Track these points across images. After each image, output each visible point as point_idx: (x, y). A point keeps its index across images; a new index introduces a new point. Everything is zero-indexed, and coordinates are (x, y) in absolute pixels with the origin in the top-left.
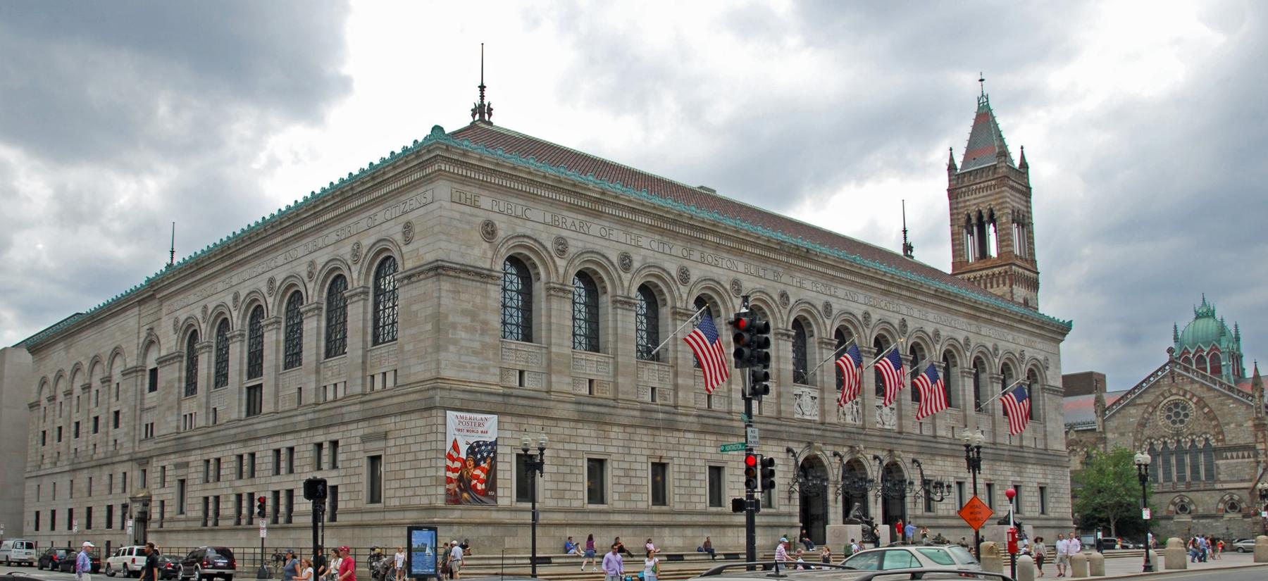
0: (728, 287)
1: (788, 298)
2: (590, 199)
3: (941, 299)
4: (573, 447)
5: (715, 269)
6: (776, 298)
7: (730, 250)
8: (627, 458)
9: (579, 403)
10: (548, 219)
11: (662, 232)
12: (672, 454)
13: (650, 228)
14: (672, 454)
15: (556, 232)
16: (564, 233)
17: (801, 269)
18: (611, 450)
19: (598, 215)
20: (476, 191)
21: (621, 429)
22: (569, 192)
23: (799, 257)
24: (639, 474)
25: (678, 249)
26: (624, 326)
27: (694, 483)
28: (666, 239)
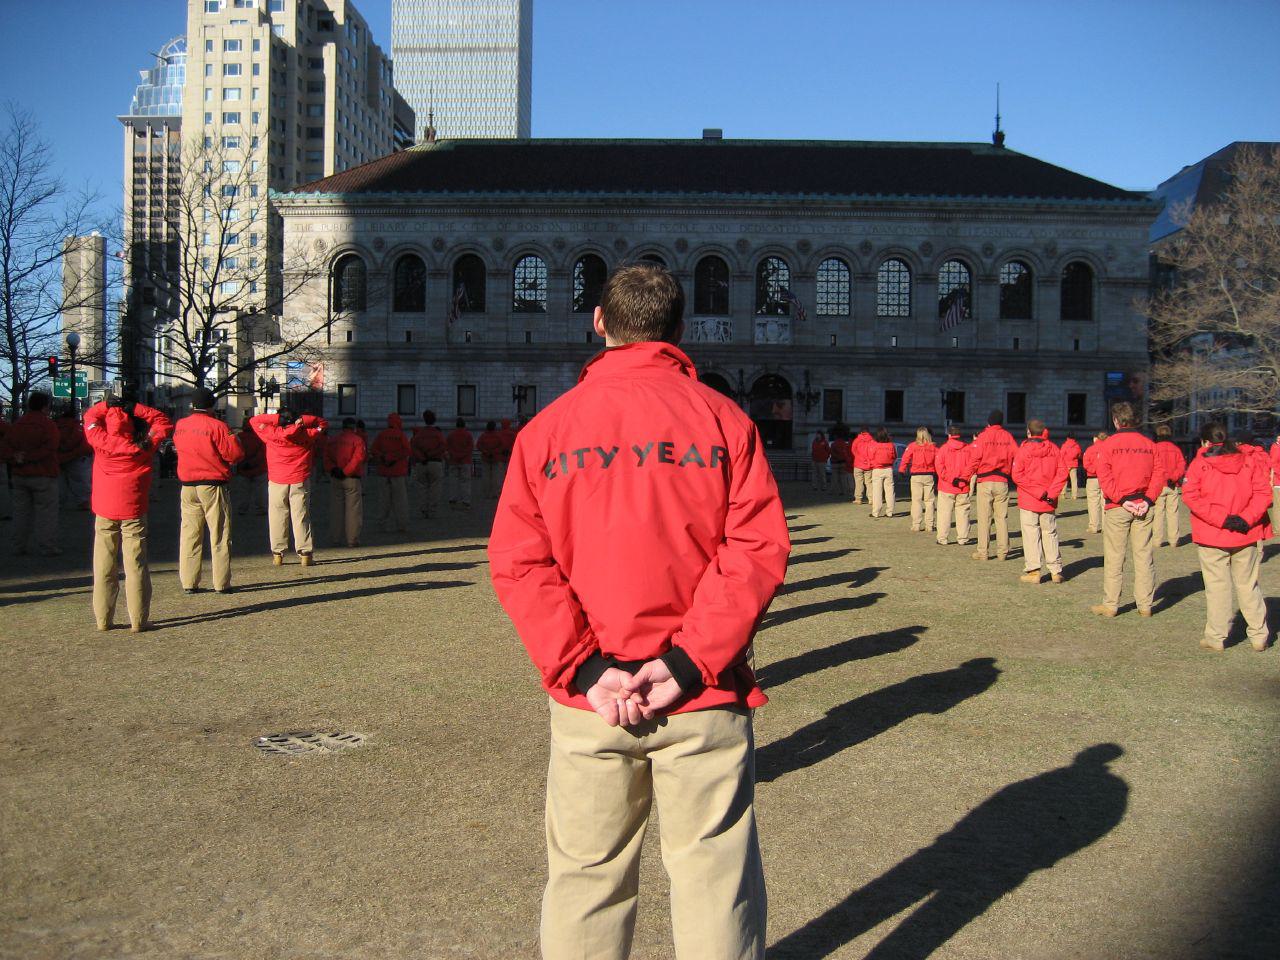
0: (549, 245)
1: (624, 243)
2: (399, 207)
3: (868, 210)
4: (386, 378)
5: (533, 234)
6: (610, 245)
7: (552, 215)
8: (434, 383)
9: (391, 349)
10: (369, 226)
11: (475, 215)
12: (476, 379)
13: (461, 215)
14: (476, 379)
15: (375, 235)
16: (382, 234)
17: (643, 215)
18: (418, 378)
19: (413, 215)
20: (309, 220)
21: (429, 364)
22: (380, 206)
23: (634, 206)
24: (445, 394)
25: (494, 224)
26: (439, 291)
27: (499, 400)
28: (480, 220)
